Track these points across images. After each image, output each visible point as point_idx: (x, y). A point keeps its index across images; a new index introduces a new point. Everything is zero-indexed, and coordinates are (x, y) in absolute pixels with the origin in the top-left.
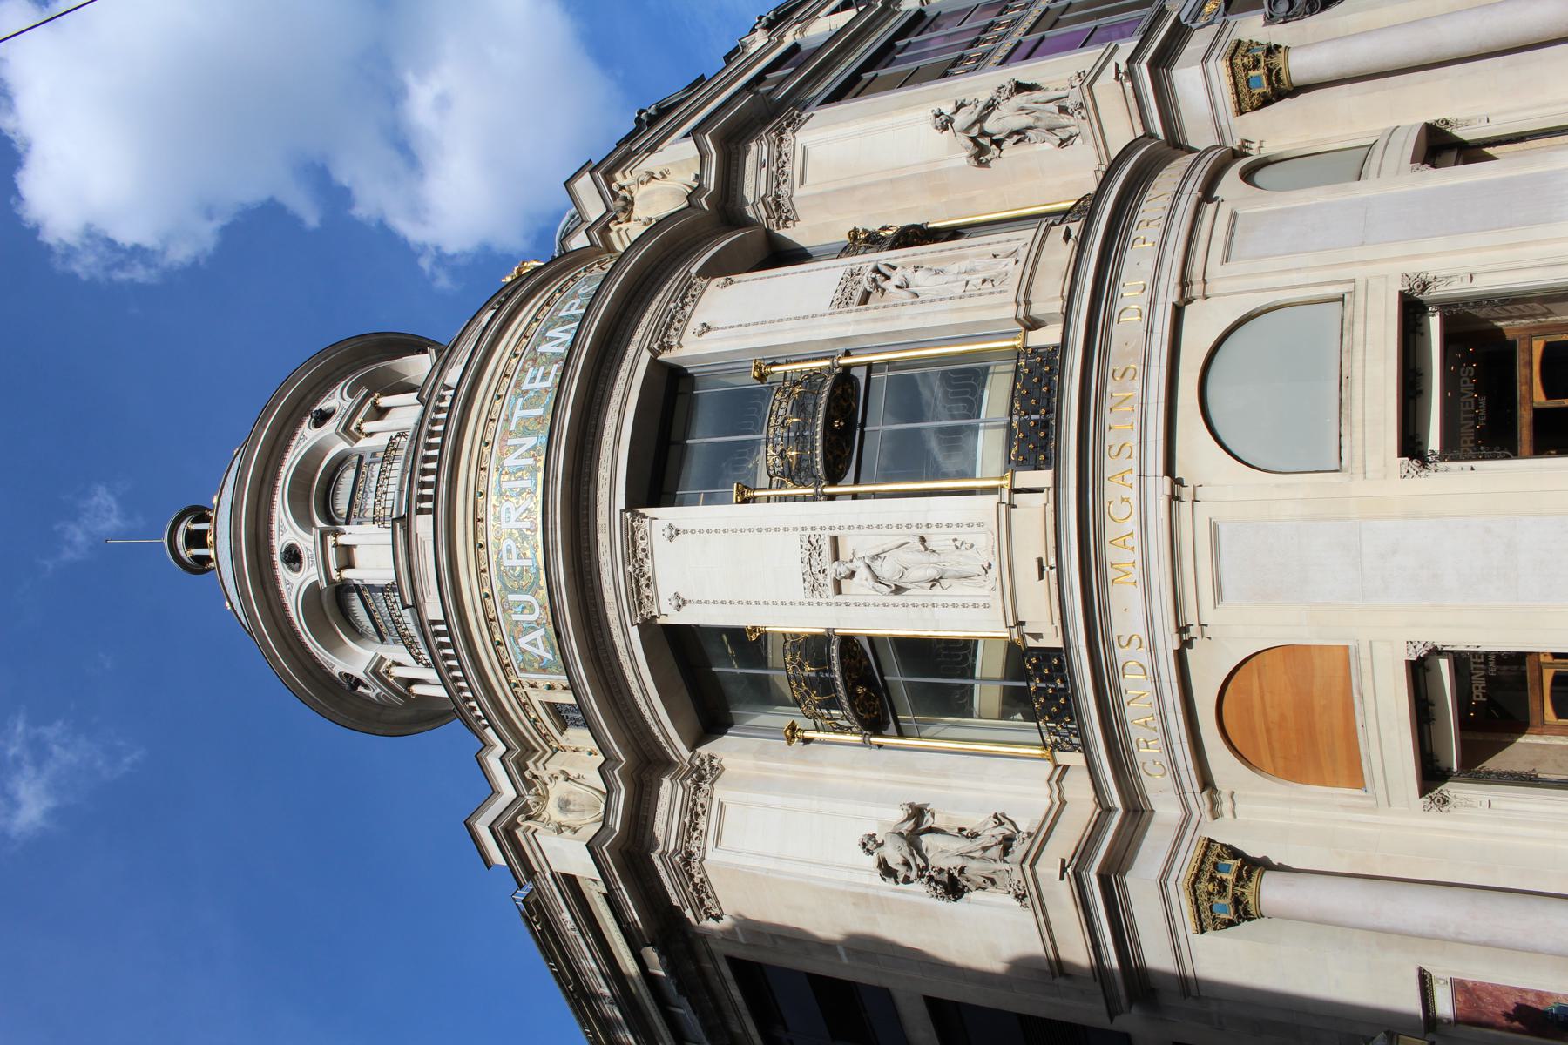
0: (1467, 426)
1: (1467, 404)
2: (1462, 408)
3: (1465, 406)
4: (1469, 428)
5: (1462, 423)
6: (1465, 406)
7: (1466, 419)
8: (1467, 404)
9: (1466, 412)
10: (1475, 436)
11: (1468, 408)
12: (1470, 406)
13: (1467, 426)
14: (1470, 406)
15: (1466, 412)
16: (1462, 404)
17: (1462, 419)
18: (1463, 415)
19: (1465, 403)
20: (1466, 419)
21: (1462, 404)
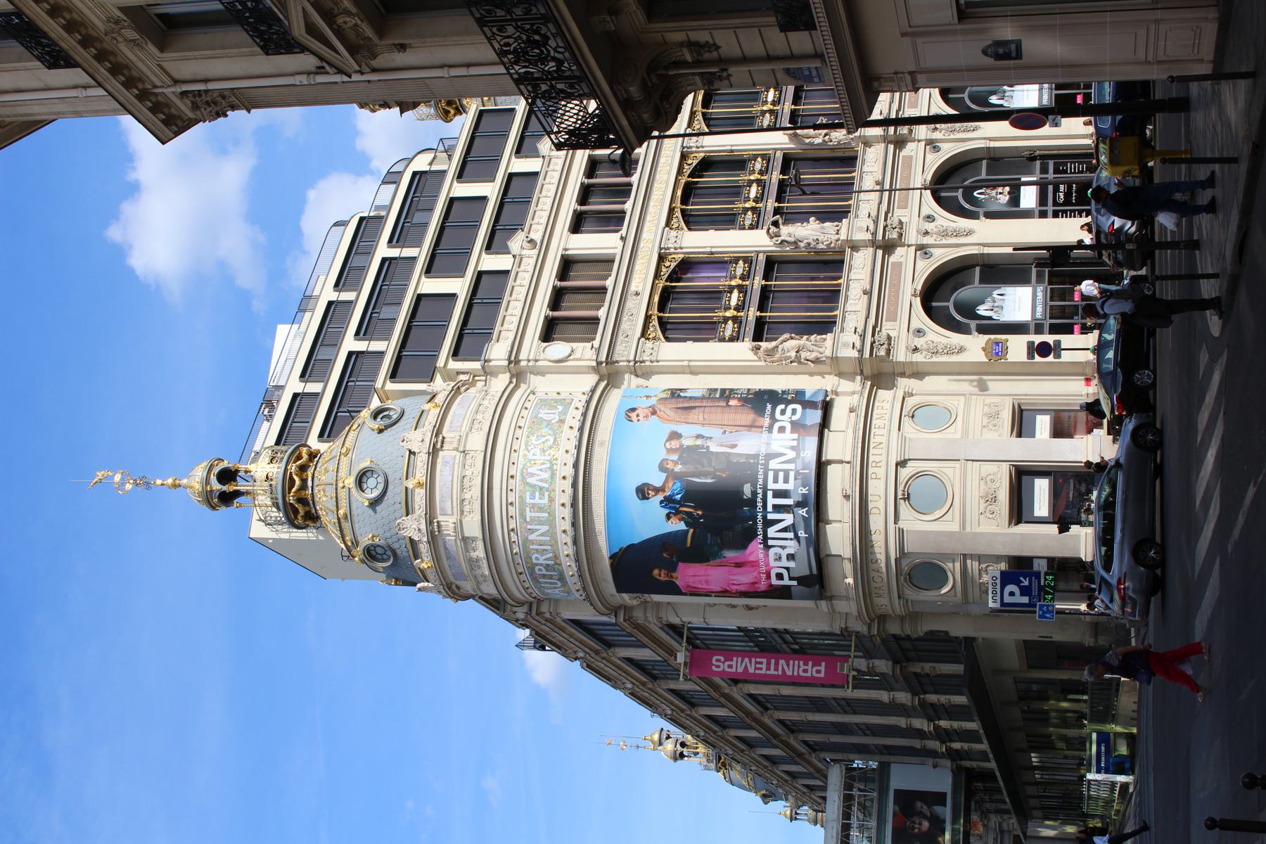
0: (785, 667)
1: (757, 666)
2: (763, 672)
3: (761, 669)
4: (788, 665)
5: (780, 673)
6: (761, 669)
7: (776, 669)
8: (757, 666)
9: (768, 668)
10: (799, 660)
11: (764, 666)
12: (761, 663)
13: (785, 667)
14: (761, 663)
15: (768, 668)
16: (757, 672)
17: (776, 673)
18: (772, 672)
19: (756, 669)
20: (776, 669)
21: (757, 672)
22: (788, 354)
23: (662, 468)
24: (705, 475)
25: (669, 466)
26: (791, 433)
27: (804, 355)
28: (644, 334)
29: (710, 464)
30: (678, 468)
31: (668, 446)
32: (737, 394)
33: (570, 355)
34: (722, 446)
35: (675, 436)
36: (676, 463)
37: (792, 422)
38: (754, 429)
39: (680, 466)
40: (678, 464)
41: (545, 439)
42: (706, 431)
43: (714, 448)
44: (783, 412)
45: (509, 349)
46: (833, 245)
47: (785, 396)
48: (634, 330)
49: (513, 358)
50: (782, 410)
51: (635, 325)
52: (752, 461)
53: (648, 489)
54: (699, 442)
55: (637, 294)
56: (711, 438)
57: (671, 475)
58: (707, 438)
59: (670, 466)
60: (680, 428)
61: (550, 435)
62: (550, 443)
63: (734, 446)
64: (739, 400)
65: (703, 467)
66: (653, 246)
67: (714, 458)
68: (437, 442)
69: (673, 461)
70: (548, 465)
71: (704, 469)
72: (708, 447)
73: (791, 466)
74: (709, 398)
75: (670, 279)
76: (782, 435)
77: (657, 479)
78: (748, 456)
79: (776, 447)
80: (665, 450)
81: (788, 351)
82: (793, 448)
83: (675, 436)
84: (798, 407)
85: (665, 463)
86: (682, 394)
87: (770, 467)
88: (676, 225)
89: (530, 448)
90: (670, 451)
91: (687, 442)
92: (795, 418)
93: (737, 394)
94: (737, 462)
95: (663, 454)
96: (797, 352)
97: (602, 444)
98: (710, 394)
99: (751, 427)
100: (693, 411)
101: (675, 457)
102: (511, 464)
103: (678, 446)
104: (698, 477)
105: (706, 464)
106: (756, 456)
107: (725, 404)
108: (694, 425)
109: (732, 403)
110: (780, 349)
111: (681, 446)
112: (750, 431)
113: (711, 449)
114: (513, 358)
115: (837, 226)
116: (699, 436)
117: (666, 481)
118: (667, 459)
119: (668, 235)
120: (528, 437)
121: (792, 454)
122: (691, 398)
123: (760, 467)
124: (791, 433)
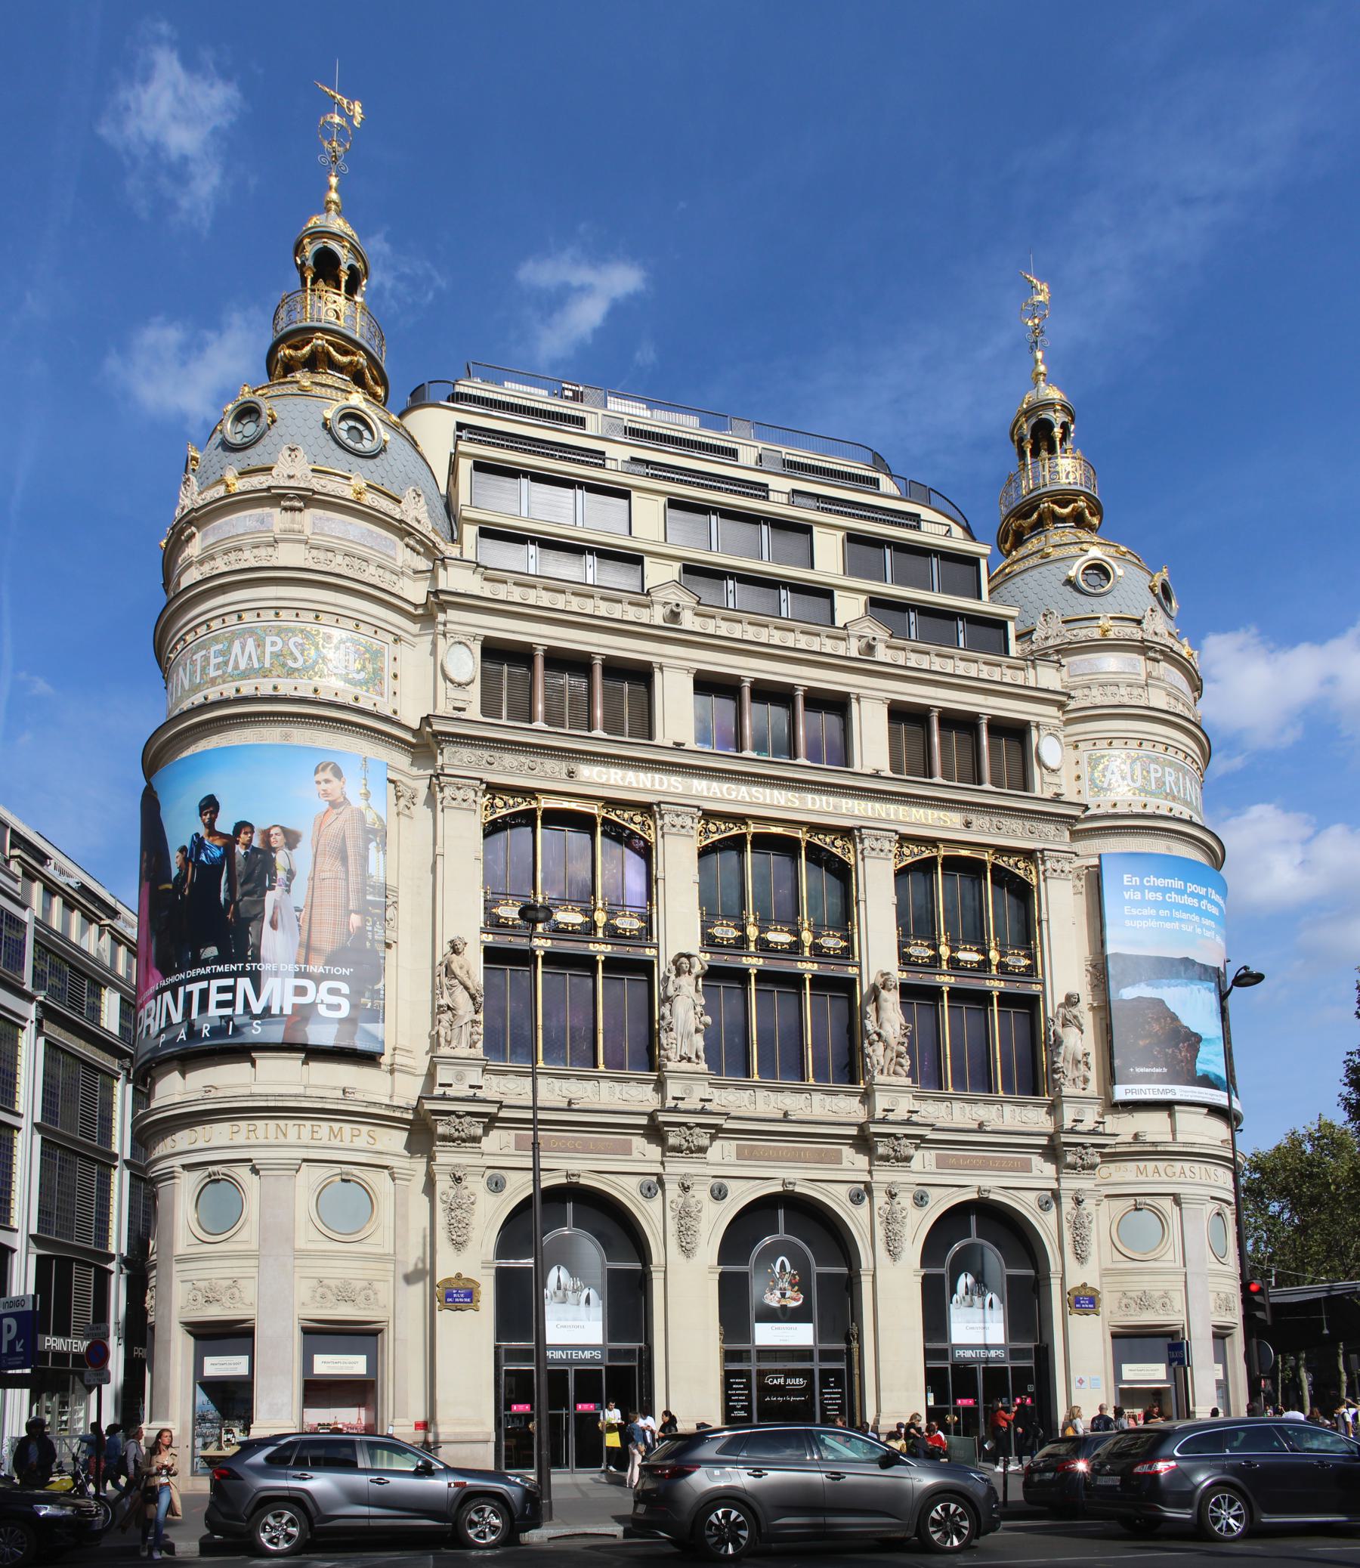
22: (446, 993)
23: (241, 826)
24: (231, 890)
25: (242, 835)
26: (294, 1005)
27: (446, 1017)
28: (493, 789)
29: (244, 895)
30: (240, 850)
31: (273, 832)
32: (374, 924)
33: (452, 682)
34: (275, 908)
35: (292, 839)
36: (247, 845)
37: (314, 1005)
38: (303, 952)
39: (243, 852)
40: (247, 848)
41: (297, 654)
42: (300, 885)
43: (270, 898)
44: (332, 991)
45: (459, 591)
46: (662, 1052)
47: (367, 994)
48: (499, 773)
49: (442, 597)
50: (339, 990)
51: (511, 774)
52: (249, 953)
53: (211, 813)
54: (281, 875)
55: (571, 774)
56: (288, 891)
57: (230, 841)
58: (289, 886)
59: (243, 838)
60: (304, 851)
61: (305, 661)
62: (290, 663)
63: (274, 925)
64: (362, 930)
65: (242, 885)
66: (664, 793)
67: (255, 898)
68: (291, 499)
69: (251, 840)
70: (256, 666)
71: (238, 887)
72: (272, 888)
73: (240, 1008)
74: (365, 884)
75: (606, 821)
76: (289, 990)
77: (225, 824)
78: (257, 948)
79: (269, 985)
80: (266, 827)
81: (451, 995)
82: (267, 1010)
83: (292, 839)
84: (345, 1011)
85: (248, 829)
86: (372, 846)
87: (239, 980)
88: (712, 828)
89: (283, 635)
90: (266, 835)
91: (281, 859)
92: (322, 1010)
93: (374, 924)
94: (249, 932)
95: (259, 825)
96: (449, 1008)
97: (287, 736)
98: (370, 886)
99: (308, 948)
100: (338, 863)
101: (256, 842)
102: (257, 611)
103: (274, 845)
104: (228, 880)
105: (248, 887)
106: (257, 958)
107: (351, 907)
108: (310, 866)
109: (355, 920)
110: (455, 982)
111: (274, 850)
112: (300, 945)
113: (269, 893)
114: (442, 597)
115: (698, 1057)
116: (291, 874)
117: (222, 835)
118: (252, 832)
119: (687, 814)
120: (302, 631)
121: (257, 1008)
122: (365, 859)
123: (240, 965)
124: (294, 1005)
